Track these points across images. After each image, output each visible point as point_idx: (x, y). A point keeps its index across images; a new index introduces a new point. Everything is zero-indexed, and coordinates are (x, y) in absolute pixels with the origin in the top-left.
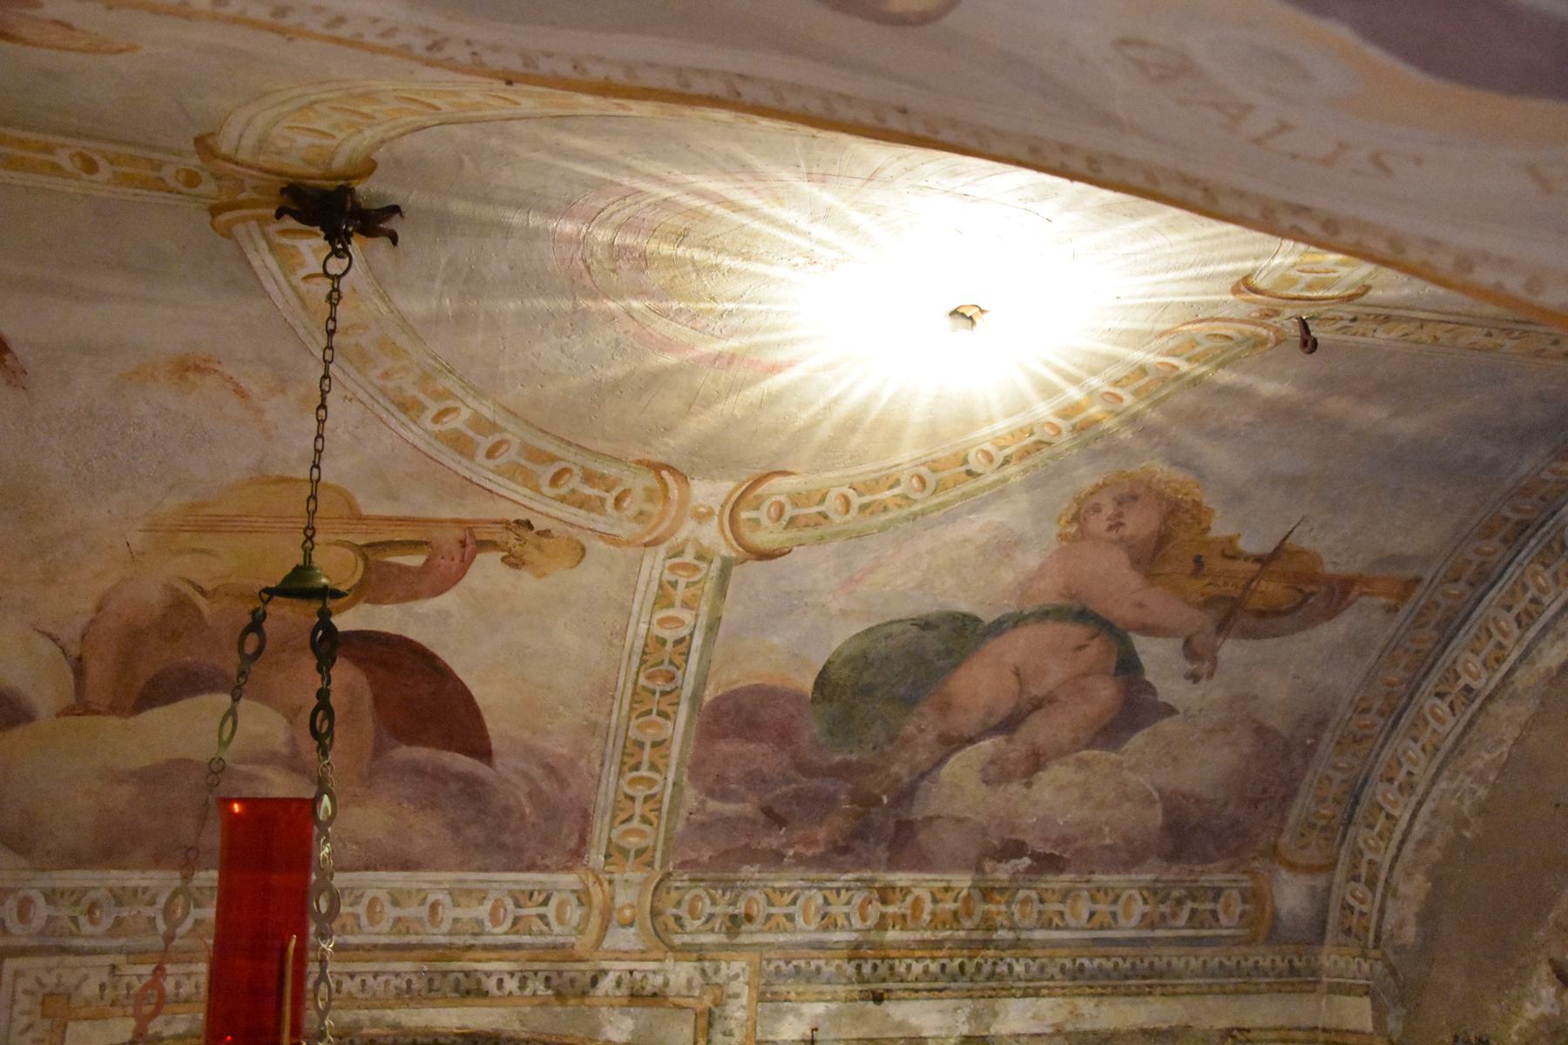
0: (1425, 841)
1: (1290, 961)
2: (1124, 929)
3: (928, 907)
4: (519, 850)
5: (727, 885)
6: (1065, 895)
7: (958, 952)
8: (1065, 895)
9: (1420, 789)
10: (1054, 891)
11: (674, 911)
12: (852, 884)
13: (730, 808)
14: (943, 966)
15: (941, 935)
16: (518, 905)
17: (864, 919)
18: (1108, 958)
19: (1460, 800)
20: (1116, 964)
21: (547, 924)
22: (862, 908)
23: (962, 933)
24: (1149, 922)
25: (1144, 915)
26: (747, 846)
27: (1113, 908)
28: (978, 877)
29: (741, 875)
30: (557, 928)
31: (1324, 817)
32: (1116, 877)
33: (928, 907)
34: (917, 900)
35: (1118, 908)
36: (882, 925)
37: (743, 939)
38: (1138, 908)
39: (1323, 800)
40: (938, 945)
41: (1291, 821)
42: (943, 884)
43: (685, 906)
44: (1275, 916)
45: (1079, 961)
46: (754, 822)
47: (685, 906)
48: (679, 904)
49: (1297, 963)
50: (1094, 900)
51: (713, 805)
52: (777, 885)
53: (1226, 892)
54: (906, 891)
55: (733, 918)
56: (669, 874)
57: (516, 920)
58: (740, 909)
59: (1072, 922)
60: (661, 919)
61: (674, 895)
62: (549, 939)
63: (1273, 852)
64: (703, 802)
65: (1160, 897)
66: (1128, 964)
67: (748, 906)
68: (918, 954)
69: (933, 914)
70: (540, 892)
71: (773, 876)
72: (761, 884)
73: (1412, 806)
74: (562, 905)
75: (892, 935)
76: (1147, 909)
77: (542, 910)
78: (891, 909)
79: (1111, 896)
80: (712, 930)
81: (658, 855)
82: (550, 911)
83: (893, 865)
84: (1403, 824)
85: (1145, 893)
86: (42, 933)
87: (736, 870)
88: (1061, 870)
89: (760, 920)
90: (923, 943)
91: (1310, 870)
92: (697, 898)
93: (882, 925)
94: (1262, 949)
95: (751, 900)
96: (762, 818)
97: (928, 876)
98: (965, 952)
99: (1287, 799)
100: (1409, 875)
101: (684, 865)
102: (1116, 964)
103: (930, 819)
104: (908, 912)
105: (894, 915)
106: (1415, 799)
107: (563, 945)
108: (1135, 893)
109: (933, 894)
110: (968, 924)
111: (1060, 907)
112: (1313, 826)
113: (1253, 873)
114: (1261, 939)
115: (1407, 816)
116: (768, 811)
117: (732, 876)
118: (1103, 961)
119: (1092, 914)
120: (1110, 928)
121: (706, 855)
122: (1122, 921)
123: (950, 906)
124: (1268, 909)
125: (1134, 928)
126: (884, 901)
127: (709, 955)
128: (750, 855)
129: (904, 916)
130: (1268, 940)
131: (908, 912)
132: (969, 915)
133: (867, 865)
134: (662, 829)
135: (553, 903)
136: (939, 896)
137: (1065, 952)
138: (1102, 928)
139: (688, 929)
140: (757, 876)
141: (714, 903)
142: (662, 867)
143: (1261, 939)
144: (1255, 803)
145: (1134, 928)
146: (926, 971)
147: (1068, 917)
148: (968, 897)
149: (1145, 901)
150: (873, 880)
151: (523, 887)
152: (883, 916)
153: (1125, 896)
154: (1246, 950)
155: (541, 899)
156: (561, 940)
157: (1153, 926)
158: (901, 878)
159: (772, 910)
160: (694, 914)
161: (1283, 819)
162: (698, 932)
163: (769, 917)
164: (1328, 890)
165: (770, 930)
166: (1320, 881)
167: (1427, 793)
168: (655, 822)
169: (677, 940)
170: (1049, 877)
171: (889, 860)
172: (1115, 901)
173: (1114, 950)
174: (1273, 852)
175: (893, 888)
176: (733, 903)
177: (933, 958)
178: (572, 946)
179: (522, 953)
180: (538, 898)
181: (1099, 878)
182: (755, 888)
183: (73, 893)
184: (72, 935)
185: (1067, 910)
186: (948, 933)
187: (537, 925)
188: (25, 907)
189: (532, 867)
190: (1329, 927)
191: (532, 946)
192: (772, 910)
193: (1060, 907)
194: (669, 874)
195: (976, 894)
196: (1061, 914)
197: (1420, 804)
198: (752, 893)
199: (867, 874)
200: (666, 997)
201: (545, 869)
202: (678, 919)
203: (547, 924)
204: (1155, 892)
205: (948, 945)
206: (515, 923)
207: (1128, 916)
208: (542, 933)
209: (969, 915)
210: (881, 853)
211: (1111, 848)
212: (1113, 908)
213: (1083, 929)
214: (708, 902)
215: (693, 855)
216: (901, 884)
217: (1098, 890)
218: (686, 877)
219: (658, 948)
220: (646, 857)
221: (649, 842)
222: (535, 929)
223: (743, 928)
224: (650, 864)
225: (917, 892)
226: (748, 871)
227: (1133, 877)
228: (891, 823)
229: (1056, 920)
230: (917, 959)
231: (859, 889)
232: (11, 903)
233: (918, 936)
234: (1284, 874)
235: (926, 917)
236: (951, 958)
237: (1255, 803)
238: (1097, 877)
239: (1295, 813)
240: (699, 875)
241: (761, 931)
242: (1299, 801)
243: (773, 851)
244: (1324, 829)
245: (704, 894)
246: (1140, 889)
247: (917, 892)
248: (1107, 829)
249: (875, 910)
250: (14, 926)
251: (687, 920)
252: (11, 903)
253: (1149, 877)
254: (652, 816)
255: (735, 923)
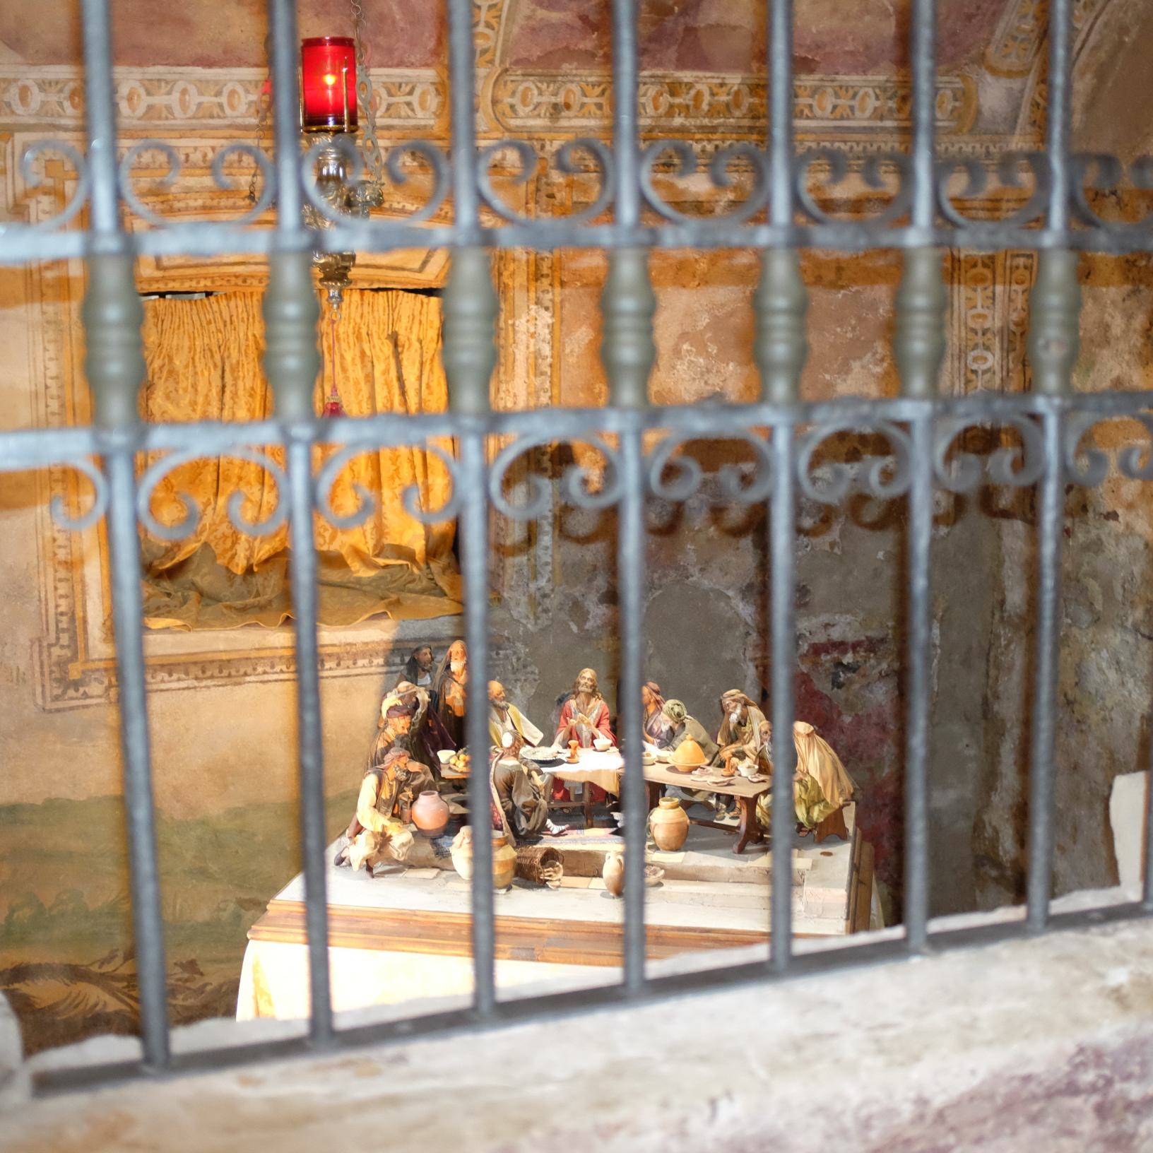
0: (1096, 48)
1: (987, 148)
2: (859, 119)
3: (707, 98)
4: (390, 51)
5: (552, 79)
6: (815, 91)
7: (728, 136)
8: (815, 91)
9: (1098, 7)
10: (806, 88)
11: (510, 100)
12: (648, 80)
13: (555, 16)
14: (717, 147)
15: (716, 122)
16: (390, 94)
17: (656, 108)
18: (845, 142)
19: (1126, 12)
20: (852, 148)
21: (413, 110)
22: (655, 99)
23: (732, 120)
24: (878, 115)
25: (876, 109)
26: (567, 47)
27: (852, 103)
28: (746, 75)
29: (562, 72)
30: (420, 114)
31: (1024, 31)
32: (855, 77)
33: (707, 98)
34: (698, 96)
35: (855, 103)
36: (670, 113)
37: (564, 123)
38: (872, 103)
39: (1025, 16)
40: (713, 130)
41: (998, 34)
42: (719, 81)
43: (518, 95)
44: (979, 112)
45: (822, 144)
46: (573, 28)
47: (518, 95)
48: (513, 94)
49: (992, 149)
50: (837, 96)
51: (541, 13)
52: (590, 79)
53: (942, 92)
54: (690, 86)
55: (555, 106)
56: (506, 70)
57: (389, 106)
58: (560, 99)
59: (818, 112)
60: (499, 106)
61: (510, 86)
62: (413, 122)
63: (981, 59)
64: (534, 11)
65: (889, 94)
66: (861, 148)
67: (567, 96)
68: (698, 136)
69: (710, 104)
70: (407, 84)
71: (586, 72)
72: (577, 79)
73: (1091, 20)
74: (423, 94)
75: (678, 121)
76: (878, 104)
77: (408, 98)
78: (677, 101)
79: (851, 92)
80: (539, 116)
81: (498, 54)
82: (415, 99)
83: (682, 64)
84: (1082, 36)
85: (878, 91)
86: (38, 114)
87: (558, 67)
88: (811, 71)
89: (575, 107)
90: (702, 128)
91: (1010, 74)
92: (528, 89)
93: (670, 113)
94: (966, 138)
95: (569, 91)
96: (579, 23)
97: (709, 74)
98: (734, 136)
99: (996, 15)
100: (1082, 74)
101: (517, 62)
102: (852, 148)
103: (711, 26)
104: (691, 103)
105: (679, 106)
106: (1094, 14)
107: (425, 126)
108: (870, 91)
109: (711, 89)
110: (737, 113)
111: (810, 101)
112: (1014, 38)
113: (964, 78)
114: (965, 130)
115: (1086, 28)
116: (584, 18)
117: (554, 72)
118: (842, 146)
119: (835, 107)
120: (848, 118)
121: (536, 52)
122: (858, 114)
123: (724, 98)
124: (973, 106)
125: (869, 119)
126: (673, 94)
127: (536, 136)
128: (569, 54)
129: (687, 107)
130: (971, 131)
131: (691, 103)
132: (738, 106)
133: (660, 64)
134: (502, 32)
135: (417, 92)
136: (715, 90)
137: (812, 137)
138: (842, 118)
139: (521, 113)
140: (574, 72)
141: (541, 94)
142: (502, 62)
143: (965, 130)
144: (970, 17)
145: (869, 119)
146: (703, 151)
147: (816, 109)
148: (737, 93)
149: (877, 98)
150: (664, 77)
151: (394, 80)
152: (671, 106)
153: (861, 93)
154: (954, 138)
155: (408, 89)
156: (423, 123)
157: (882, 118)
158: (686, 76)
159: (586, 100)
160: (524, 102)
161: (992, 33)
162: (528, 117)
163: (583, 105)
164: (1022, 91)
165: (583, 117)
166: (1016, 84)
167: (1103, 8)
168: (496, 25)
169: (513, 122)
170: (803, 77)
171: (678, 60)
172: (854, 97)
173: (847, 137)
174: (981, 59)
175: (680, 83)
176: (555, 94)
177: (709, 140)
178: (432, 127)
179: (393, 133)
180: (406, 89)
181: (842, 78)
182: (572, 82)
183: (57, 83)
184: (60, 116)
185: (815, 104)
186: (722, 120)
187: (404, 111)
188: (24, 93)
189: (399, 65)
190: (1020, 121)
191: (403, 128)
192: (586, 100)
193: (810, 101)
194: (506, 70)
195: (745, 90)
196: (811, 106)
197: (1096, 18)
198: (569, 86)
199: (659, 72)
200: (503, 168)
201: (411, 65)
202: (512, 107)
203: (413, 110)
204: (884, 90)
205: (721, 129)
206: (388, 109)
207: (863, 110)
208: (409, 117)
209: (738, 106)
210: (672, 53)
211: (851, 53)
212: (852, 103)
213: (828, 119)
214: (536, 92)
215: (524, 54)
216: (686, 80)
217: (841, 87)
218: (519, 72)
219: (498, 130)
220: (488, 56)
221: (491, 44)
222: (403, 113)
223: (563, 114)
224: (491, 62)
225: (698, 87)
226: (566, 67)
227: (870, 78)
228: (681, 29)
229: (806, 111)
230: (697, 141)
231: (652, 83)
232: (14, 91)
233: (698, 122)
234: (989, 78)
235: (705, 107)
236: (723, 140)
237: (970, 17)
238: (839, 77)
239: (1001, 29)
240: (530, 71)
241: (576, 117)
242: (1006, 18)
243: (586, 51)
244: (1023, 40)
245: (533, 87)
246: (873, 88)
247: (698, 87)
248: (850, 38)
249: (666, 99)
250: (19, 109)
251: (521, 110)
252: (14, 91)
253: (882, 78)
254: (493, 22)
255: (556, 110)
